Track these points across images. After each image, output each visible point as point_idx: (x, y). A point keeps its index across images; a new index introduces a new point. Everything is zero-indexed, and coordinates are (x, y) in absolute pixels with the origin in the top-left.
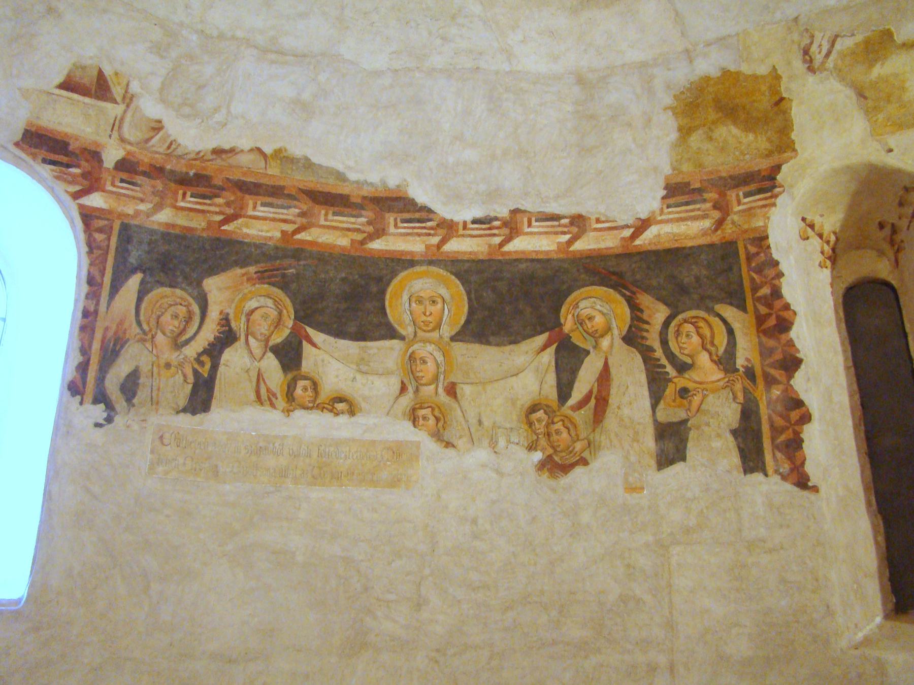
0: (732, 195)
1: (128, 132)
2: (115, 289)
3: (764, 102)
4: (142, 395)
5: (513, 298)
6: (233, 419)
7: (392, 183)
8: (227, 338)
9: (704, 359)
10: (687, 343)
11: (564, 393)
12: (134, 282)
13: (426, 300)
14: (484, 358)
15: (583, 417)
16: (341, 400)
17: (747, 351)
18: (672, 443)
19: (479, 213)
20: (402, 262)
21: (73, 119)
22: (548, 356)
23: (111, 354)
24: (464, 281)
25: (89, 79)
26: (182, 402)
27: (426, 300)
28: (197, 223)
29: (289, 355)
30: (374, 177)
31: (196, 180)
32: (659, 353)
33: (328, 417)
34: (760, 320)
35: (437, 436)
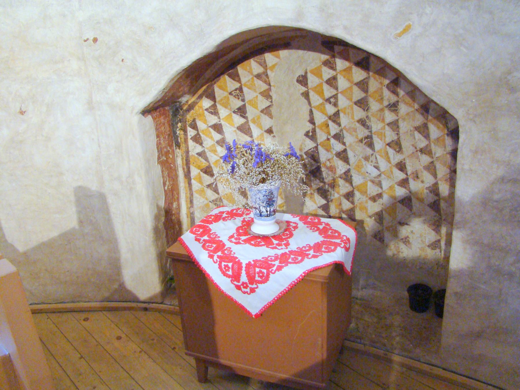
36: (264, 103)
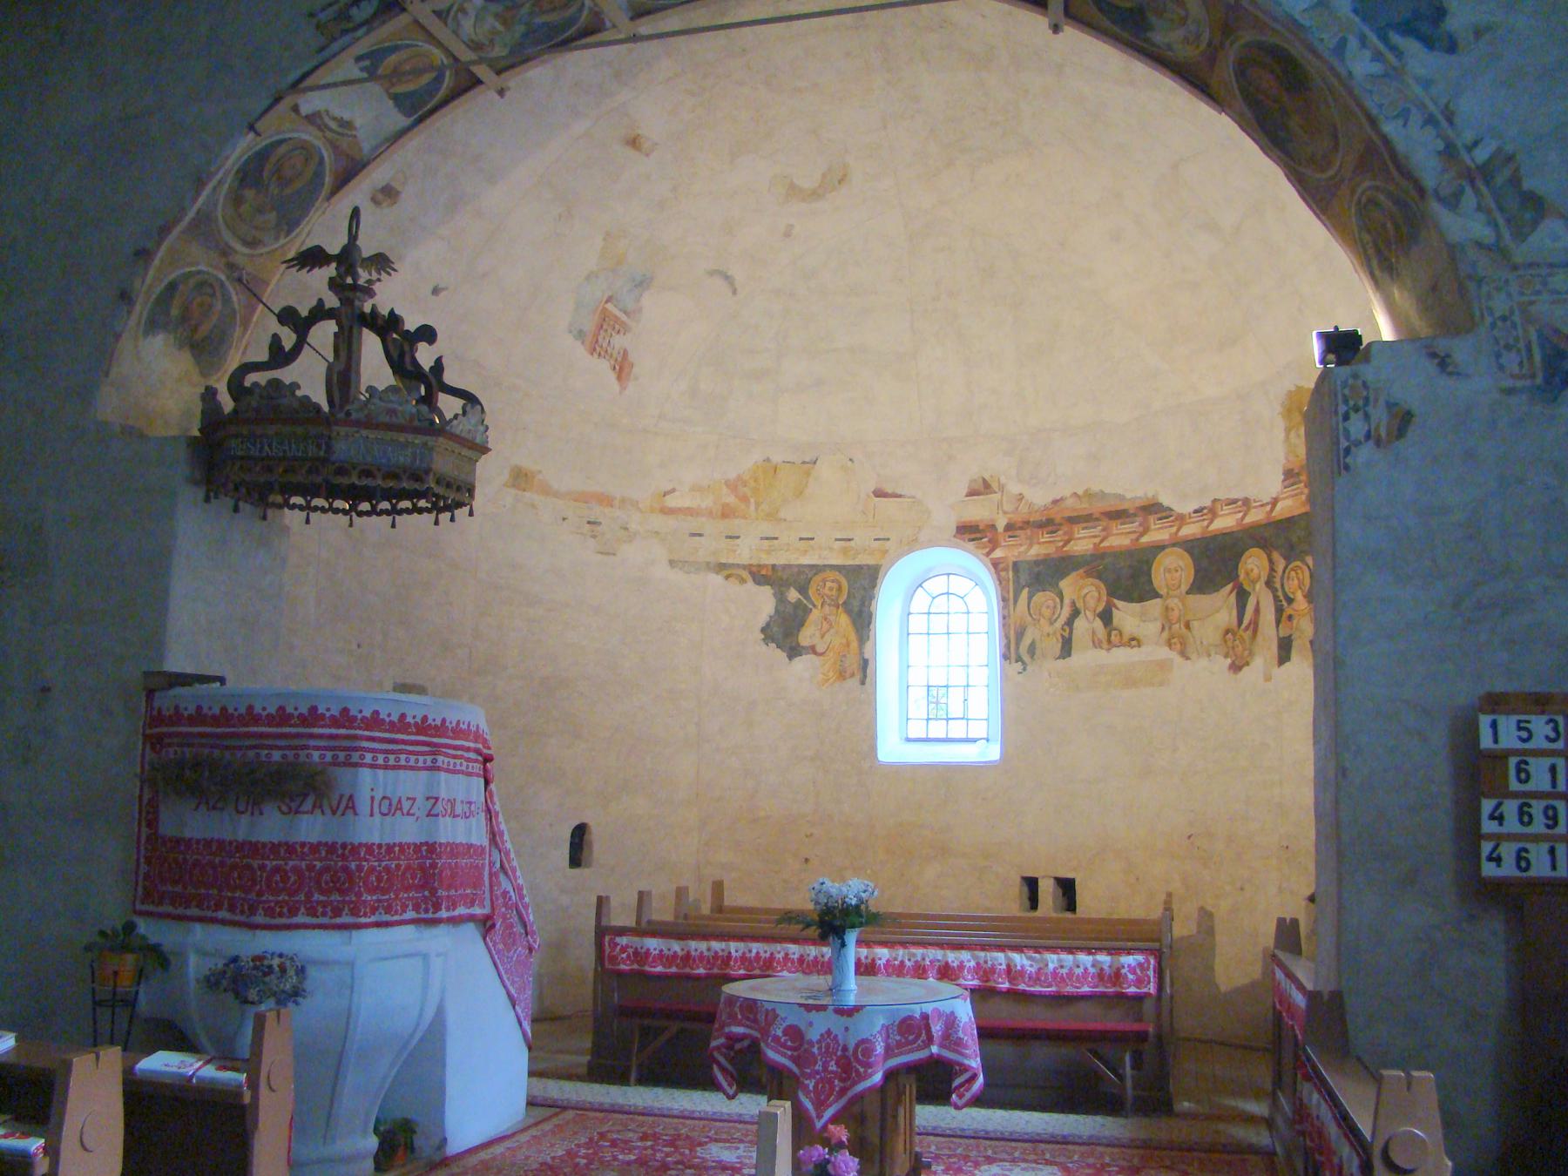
1: (1006, 507)
4: (1038, 652)
5: (1216, 561)
6: (1085, 657)
7: (1150, 495)
8: (1075, 613)
9: (1299, 596)
10: (1292, 586)
12: (1025, 592)
13: (1172, 570)
15: (1247, 635)
16: (1133, 639)
18: (1285, 650)
20: (1159, 548)
21: (979, 511)
23: (1020, 635)
24: (1191, 555)
25: (979, 486)
26: (1058, 653)
27: (1172, 570)
28: (1051, 550)
29: (1106, 617)
30: (1140, 493)
31: (1047, 524)
32: (1280, 593)
33: (1128, 650)
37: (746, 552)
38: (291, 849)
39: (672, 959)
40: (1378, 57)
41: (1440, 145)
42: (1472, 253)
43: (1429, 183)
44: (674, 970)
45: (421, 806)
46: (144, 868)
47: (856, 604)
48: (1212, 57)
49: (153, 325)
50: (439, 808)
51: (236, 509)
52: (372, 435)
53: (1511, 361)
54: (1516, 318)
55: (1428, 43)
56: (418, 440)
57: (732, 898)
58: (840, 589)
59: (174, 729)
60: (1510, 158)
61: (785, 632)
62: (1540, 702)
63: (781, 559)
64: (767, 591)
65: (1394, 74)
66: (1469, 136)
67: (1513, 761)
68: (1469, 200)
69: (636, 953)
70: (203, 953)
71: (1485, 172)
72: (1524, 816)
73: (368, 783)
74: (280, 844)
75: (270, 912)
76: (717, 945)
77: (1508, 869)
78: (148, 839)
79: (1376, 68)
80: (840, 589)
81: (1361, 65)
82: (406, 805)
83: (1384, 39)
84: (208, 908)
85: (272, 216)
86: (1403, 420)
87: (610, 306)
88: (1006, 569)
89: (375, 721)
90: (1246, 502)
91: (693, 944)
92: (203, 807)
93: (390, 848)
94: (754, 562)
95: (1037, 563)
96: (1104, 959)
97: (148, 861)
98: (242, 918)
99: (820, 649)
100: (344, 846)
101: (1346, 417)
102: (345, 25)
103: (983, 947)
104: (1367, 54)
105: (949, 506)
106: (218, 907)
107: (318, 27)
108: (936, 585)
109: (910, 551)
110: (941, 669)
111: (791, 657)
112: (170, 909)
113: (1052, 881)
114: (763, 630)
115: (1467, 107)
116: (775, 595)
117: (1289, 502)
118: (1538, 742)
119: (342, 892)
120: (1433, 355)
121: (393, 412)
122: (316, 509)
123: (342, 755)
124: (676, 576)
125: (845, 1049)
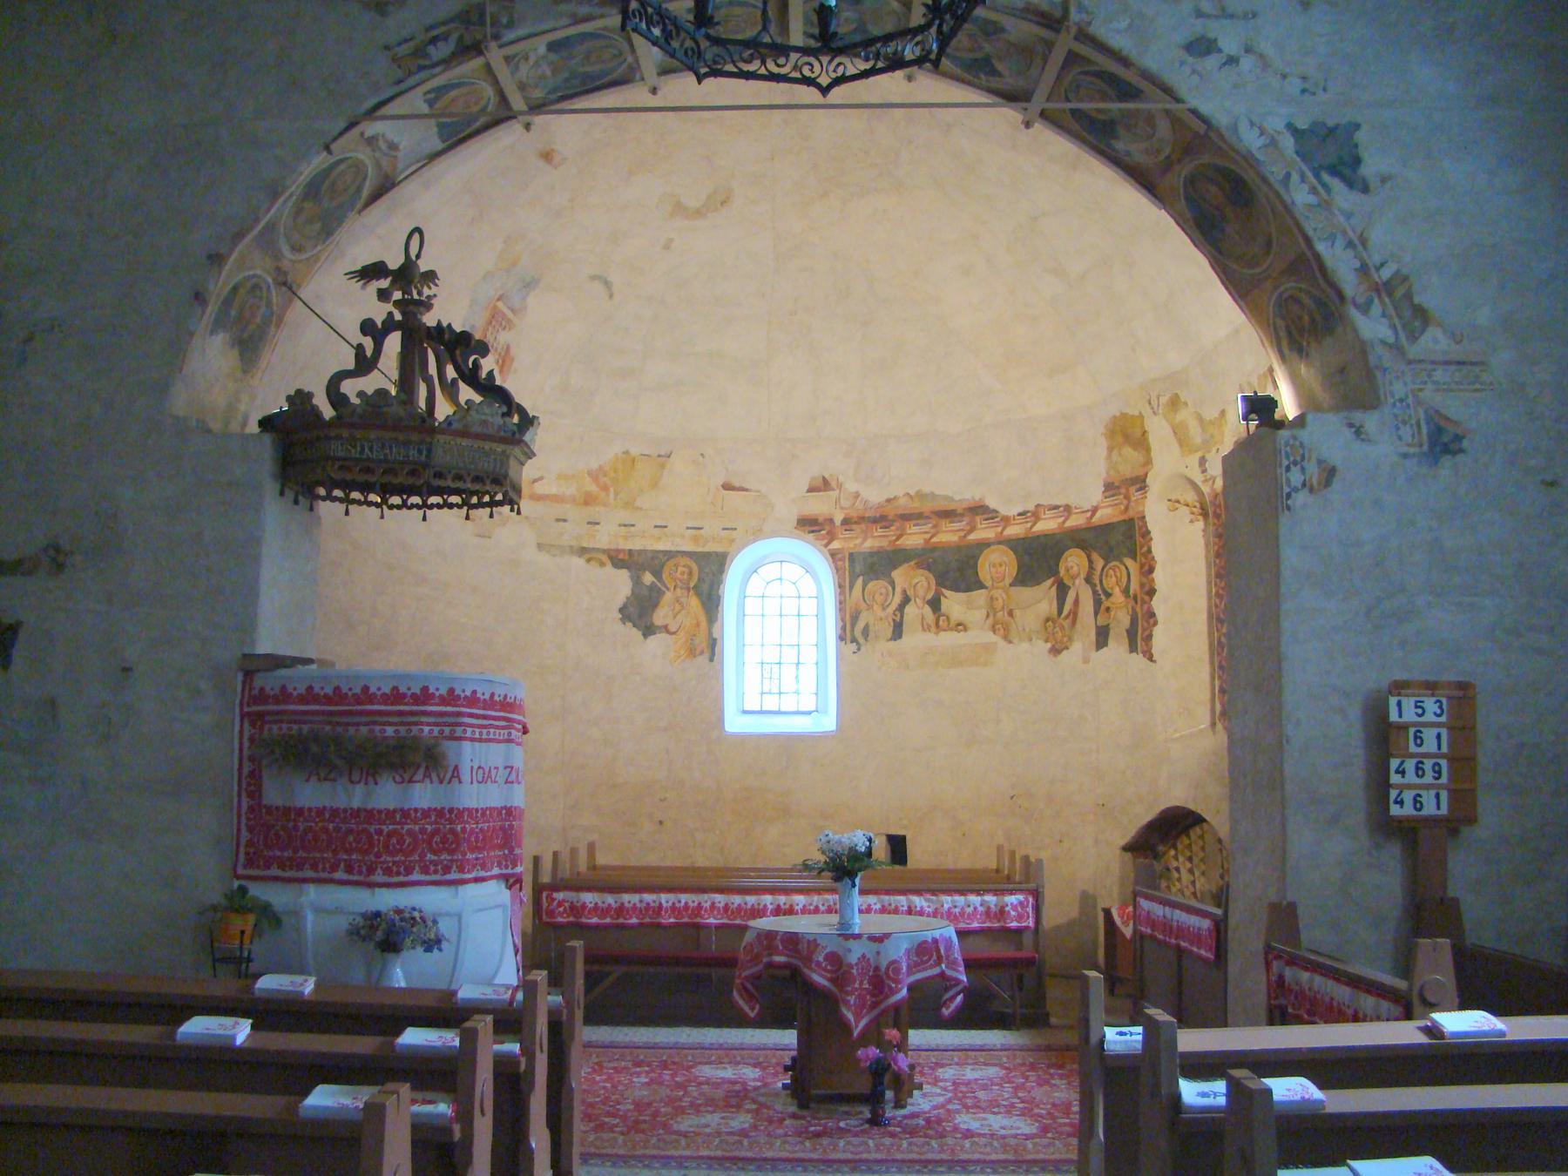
0: (1133, 489)
1: (844, 503)
2: (851, 588)
3: (1138, 433)
4: (871, 634)
6: (914, 639)
8: (906, 600)
9: (1117, 590)
10: (1110, 582)
11: (1060, 611)
12: (860, 581)
13: (997, 565)
14: (1026, 593)
15: (1066, 624)
17: (1134, 586)
19: (1021, 510)
20: (984, 545)
21: (819, 506)
22: (1054, 588)
23: (855, 618)
28: (884, 543)
29: (935, 604)
30: (968, 496)
34: (1142, 566)
35: (1006, 638)
36: (1201, 854)
37: (606, 536)
38: (405, 813)
39: (605, 911)
40: (1313, 191)
41: (1358, 265)
42: (1380, 350)
43: (1349, 291)
44: (608, 920)
45: (503, 773)
46: (245, 834)
47: (705, 587)
48: (1167, 166)
49: (218, 325)
50: (513, 777)
51: (296, 502)
52: (465, 442)
53: (1406, 432)
54: (1410, 400)
55: (1350, 184)
56: (500, 448)
57: (602, 859)
58: (690, 573)
59: (282, 707)
60: (1406, 279)
61: (640, 613)
62: (1431, 687)
63: (636, 545)
64: (624, 574)
65: (1326, 205)
66: (1376, 259)
67: (1412, 731)
68: (1376, 309)
69: (573, 908)
70: (318, 910)
71: (1386, 289)
72: (1419, 770)
73: (468, 755)
74: (395, 811)
75: (388, 872)
76: (649, 897)
77: (1408, 810)
78: (251, 809)
79: (1312, 199)
80: (690, 573)
81: (1300, 196)
82: (493, 772)
83: (1317, 176)
84: (324, 870)
85: (317, 226)
86: (1330, 473)
87: (500, 305)
88: (842, 559)
89: (473, 700)
90: (1068, 508)
91: (626, 898)
92: (314, 778)
93: (484, 811)
94: (613, 547)
95: (872, 554)
96: (991, 899)
97: (250, 830)
98: (361, 878)
99: (673, 629)
100: (451, 810)
101: (1288, 469)
102: (422, 62)
103: (888, 893)
104: (1306, 187)
105: (791, 501)
106: (334, 868)
107: (394, 60)
108: (769, 571)
109: (755, 541)
110: (781, 649)
111: (645, 635)
112: (280, 873)
113: (884, 839)
114: (621, 610)
115: (1376, 236)
116: (632, 578)
117: (1109, 511)
118: (1429, 717)
119: (452, 852)
120: (1351, 425)
121: (485, 422)
122: (354, 502)
123: (447, 730)
124: (544, 558)
125: (877, 968)
